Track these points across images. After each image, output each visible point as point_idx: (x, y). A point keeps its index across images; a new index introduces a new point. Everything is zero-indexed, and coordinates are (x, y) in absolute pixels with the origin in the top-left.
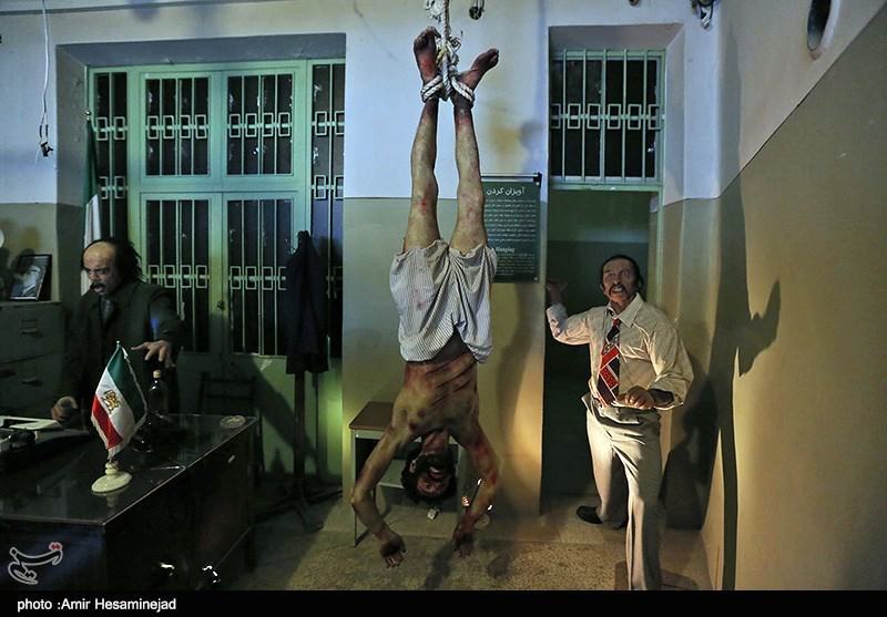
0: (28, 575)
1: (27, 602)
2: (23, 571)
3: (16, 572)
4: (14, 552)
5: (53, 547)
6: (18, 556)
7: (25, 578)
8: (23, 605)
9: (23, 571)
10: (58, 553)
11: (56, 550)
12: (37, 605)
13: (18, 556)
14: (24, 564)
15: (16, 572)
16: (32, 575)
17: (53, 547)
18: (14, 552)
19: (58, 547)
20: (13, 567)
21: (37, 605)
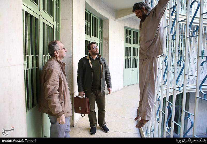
0: (6, 134)
1: (4, 140)
2: (5, 133)
3: (3, 133)
4: (3, 129)
5: (12, 128)
6: (4, 130)
7: (6, 135)
8: (3, 141)
9: (5, 133)
10: (13, 129)
11: (13, 128)
12: (7, 141)
13: (4, 130)
14: (5, 132)
15: (3, 133)
16: (7, 134)
17: (12, 128)
18: (3, 129)
19: (13, 128)
20: (3, 132)
21: (7, 141)
